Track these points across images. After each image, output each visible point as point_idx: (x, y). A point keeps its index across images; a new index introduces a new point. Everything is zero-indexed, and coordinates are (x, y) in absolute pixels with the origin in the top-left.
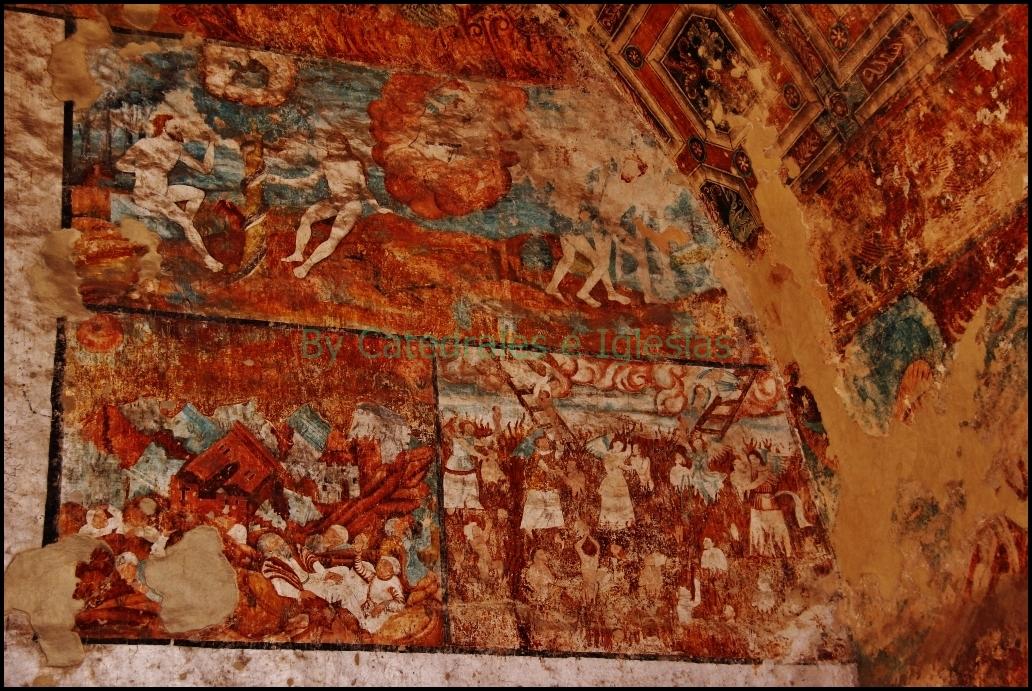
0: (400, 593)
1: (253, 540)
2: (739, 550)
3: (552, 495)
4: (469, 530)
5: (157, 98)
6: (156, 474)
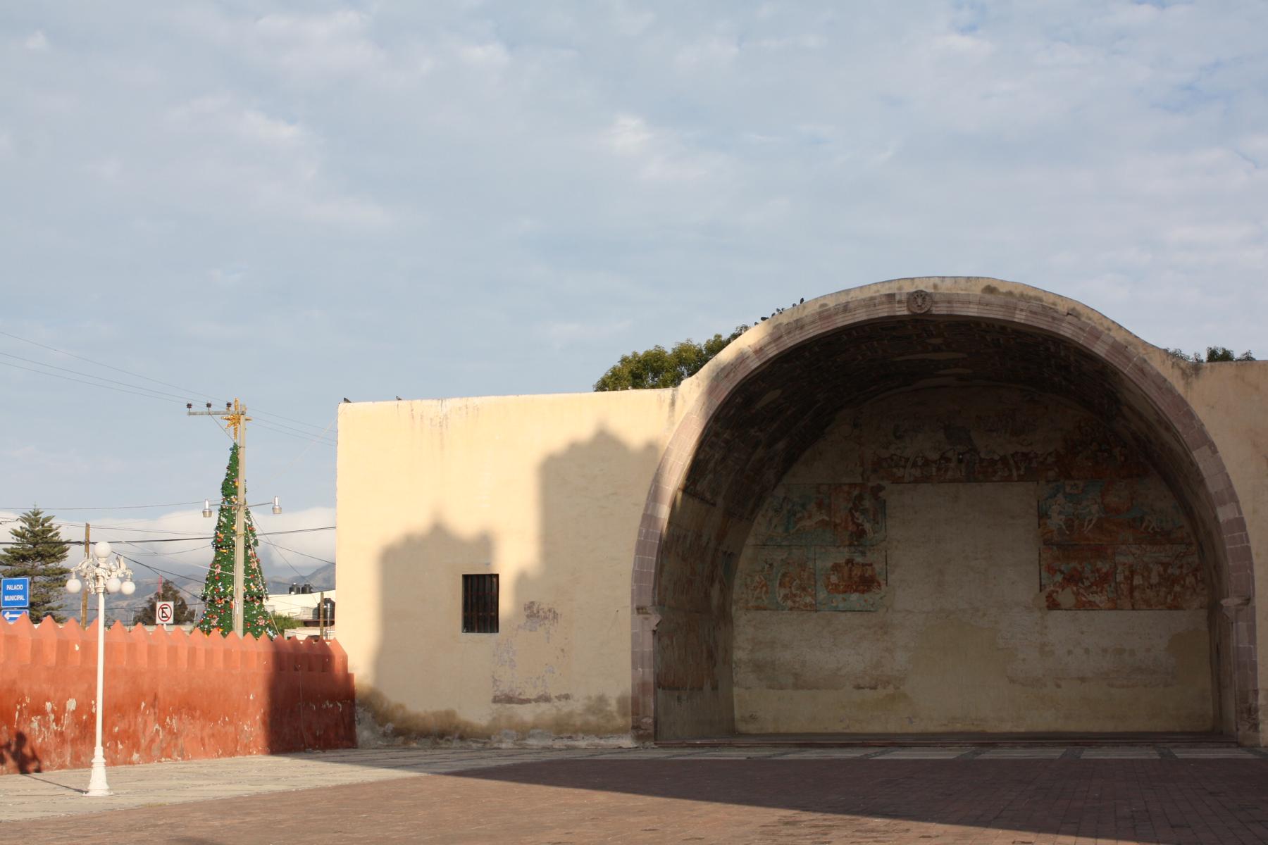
0: (1107, 599)
1: (1077, 590)
2: (1183, 586)
3: (1140, 577)
4: (1122, 585)
5: (1055, 496)
6: (1059, 578)
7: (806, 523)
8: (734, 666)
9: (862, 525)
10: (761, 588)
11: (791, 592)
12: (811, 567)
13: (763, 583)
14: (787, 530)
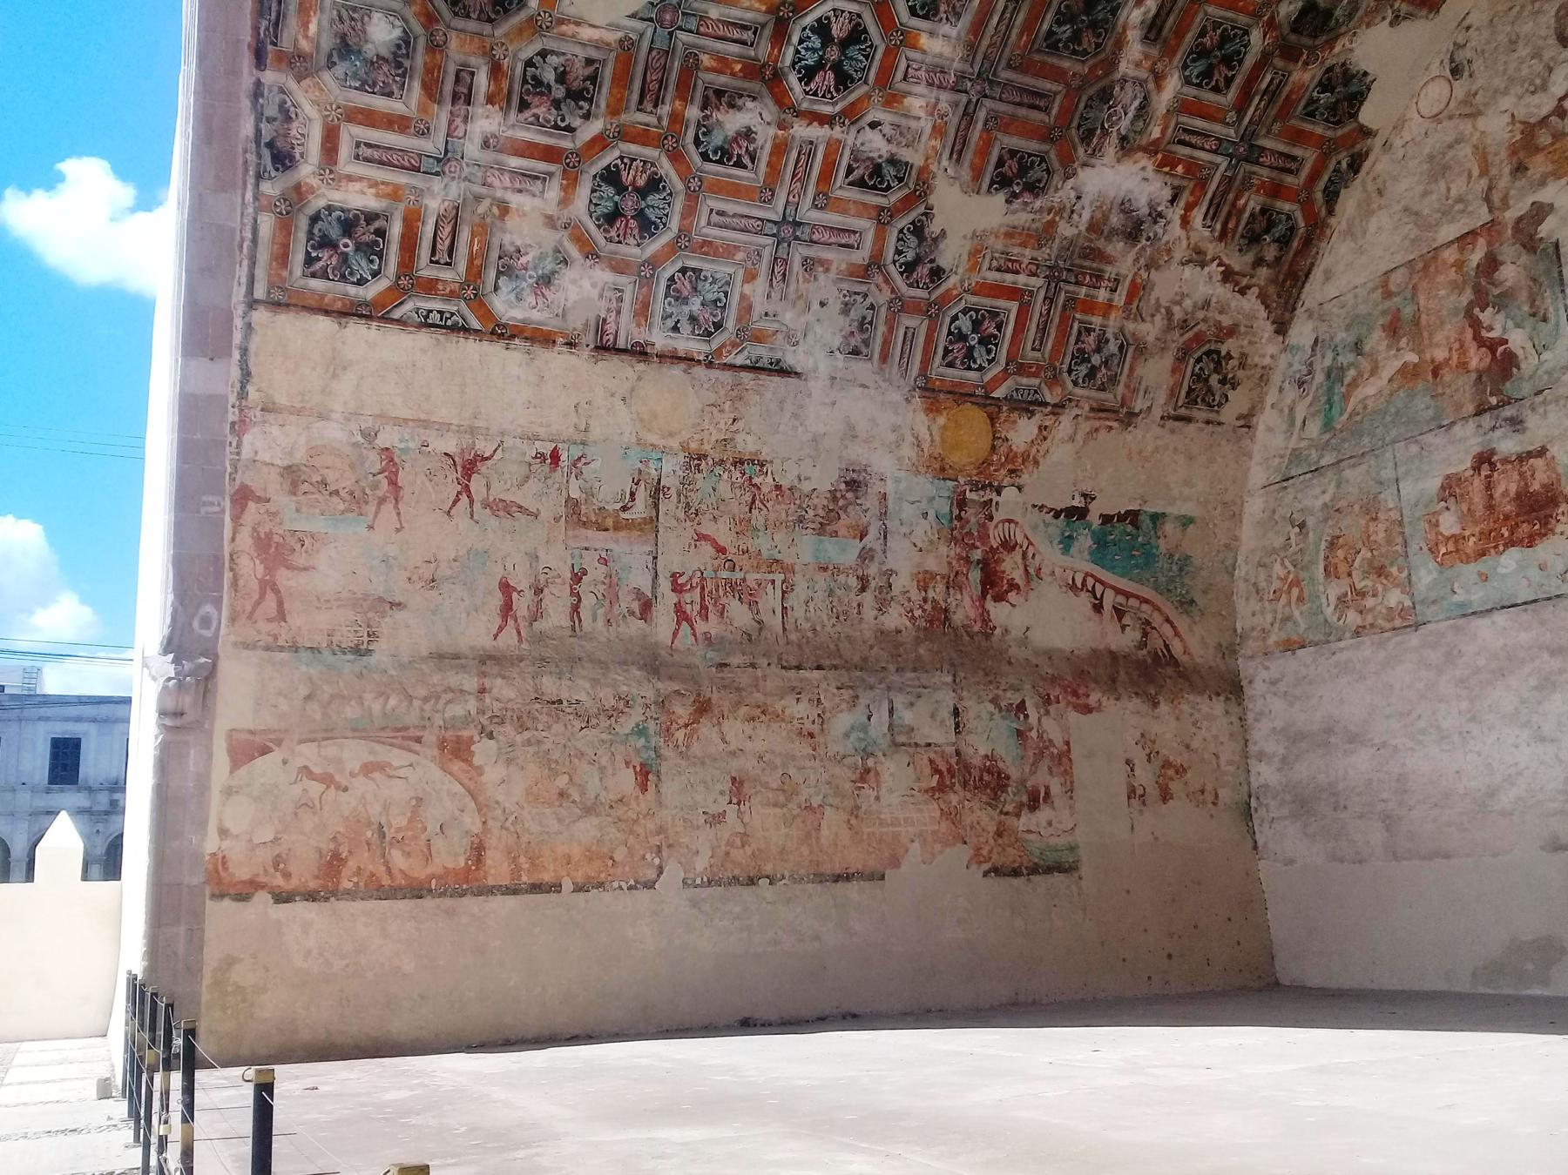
7: (1369, 389)
8: (1253, 803)
9: (1506, 342)
10: (1289, 592)
11: (1353, 586)
12: (1391, 506)
13: (1291, 577)
14: (1328, 426)
